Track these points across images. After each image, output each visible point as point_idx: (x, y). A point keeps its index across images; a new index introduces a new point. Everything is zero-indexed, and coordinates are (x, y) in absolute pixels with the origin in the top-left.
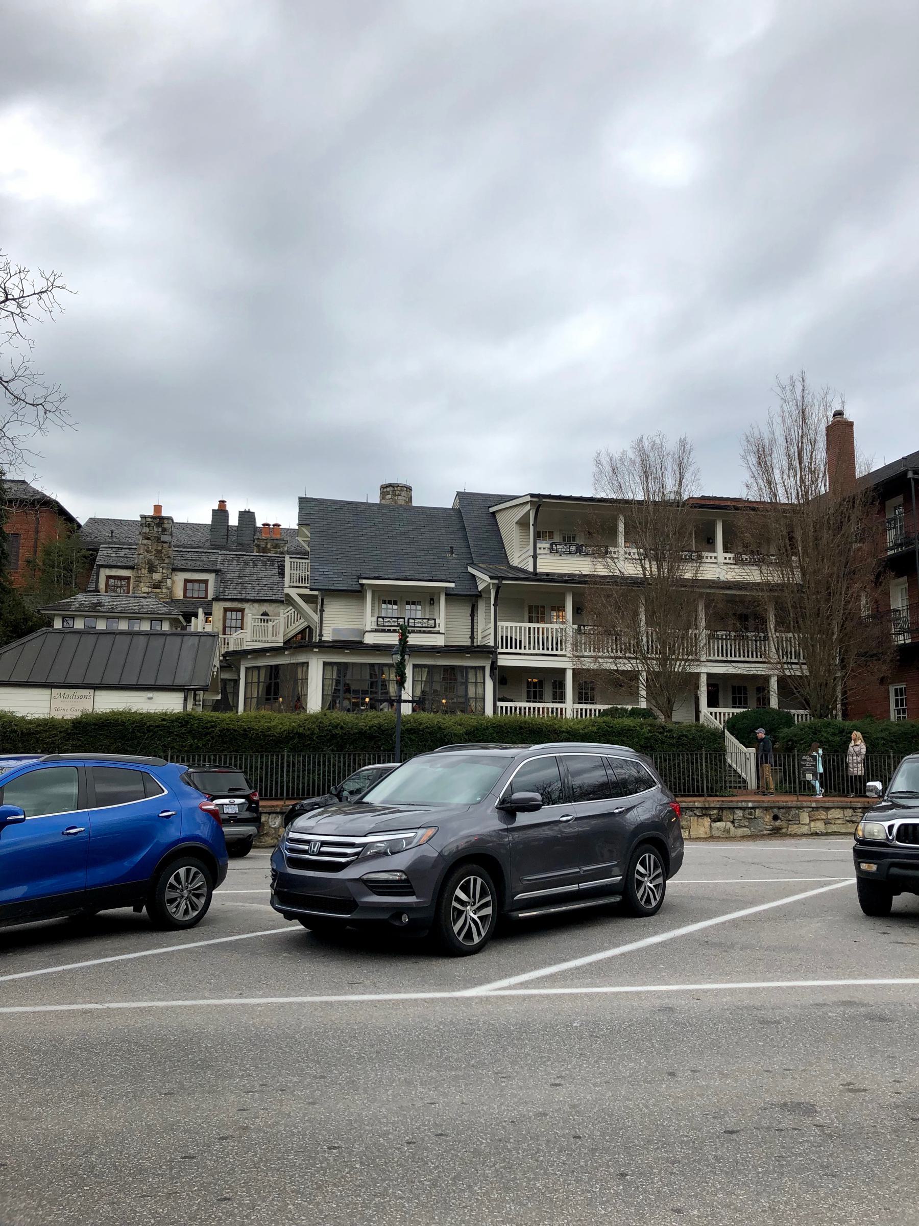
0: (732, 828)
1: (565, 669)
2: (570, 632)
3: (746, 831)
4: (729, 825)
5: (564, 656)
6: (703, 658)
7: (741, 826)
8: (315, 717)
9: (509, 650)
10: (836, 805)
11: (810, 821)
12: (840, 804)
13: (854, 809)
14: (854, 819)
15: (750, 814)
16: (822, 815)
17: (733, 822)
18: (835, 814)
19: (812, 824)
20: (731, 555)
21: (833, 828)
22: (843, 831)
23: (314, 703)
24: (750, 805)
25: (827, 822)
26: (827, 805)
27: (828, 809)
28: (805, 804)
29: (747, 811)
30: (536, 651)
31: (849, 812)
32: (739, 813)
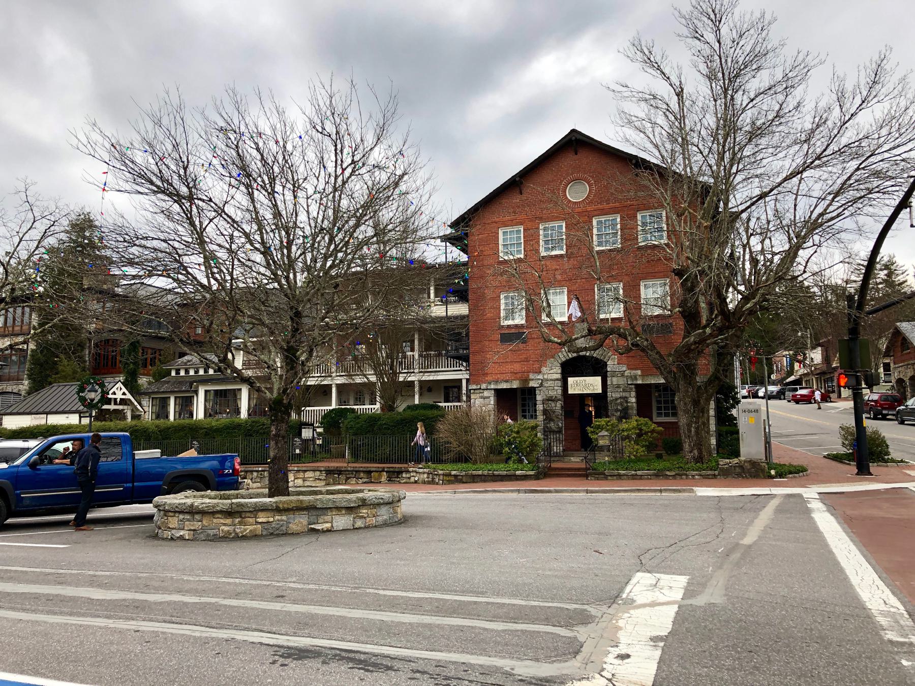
0: (251, 483)
2: (417, 357)
3: (259, 485)
5: (461, 370)
6: (334, 375)
8: (172, 424)
9: (443, 369)
10: (309, 469)
11: (295, 479)
12: (311, 468)
15: (261, 474)
16: (301, 475)
17: (252, 479)
18: (309, 474)
19: (296, 481)
23: (244, 414)
24: (260, 469)
25: (304, 480)
26: (304, 469)
27: (306, 471)
28: (255, 469)
30: (455, 369)
31: (318, 473)
32: (255, 474)
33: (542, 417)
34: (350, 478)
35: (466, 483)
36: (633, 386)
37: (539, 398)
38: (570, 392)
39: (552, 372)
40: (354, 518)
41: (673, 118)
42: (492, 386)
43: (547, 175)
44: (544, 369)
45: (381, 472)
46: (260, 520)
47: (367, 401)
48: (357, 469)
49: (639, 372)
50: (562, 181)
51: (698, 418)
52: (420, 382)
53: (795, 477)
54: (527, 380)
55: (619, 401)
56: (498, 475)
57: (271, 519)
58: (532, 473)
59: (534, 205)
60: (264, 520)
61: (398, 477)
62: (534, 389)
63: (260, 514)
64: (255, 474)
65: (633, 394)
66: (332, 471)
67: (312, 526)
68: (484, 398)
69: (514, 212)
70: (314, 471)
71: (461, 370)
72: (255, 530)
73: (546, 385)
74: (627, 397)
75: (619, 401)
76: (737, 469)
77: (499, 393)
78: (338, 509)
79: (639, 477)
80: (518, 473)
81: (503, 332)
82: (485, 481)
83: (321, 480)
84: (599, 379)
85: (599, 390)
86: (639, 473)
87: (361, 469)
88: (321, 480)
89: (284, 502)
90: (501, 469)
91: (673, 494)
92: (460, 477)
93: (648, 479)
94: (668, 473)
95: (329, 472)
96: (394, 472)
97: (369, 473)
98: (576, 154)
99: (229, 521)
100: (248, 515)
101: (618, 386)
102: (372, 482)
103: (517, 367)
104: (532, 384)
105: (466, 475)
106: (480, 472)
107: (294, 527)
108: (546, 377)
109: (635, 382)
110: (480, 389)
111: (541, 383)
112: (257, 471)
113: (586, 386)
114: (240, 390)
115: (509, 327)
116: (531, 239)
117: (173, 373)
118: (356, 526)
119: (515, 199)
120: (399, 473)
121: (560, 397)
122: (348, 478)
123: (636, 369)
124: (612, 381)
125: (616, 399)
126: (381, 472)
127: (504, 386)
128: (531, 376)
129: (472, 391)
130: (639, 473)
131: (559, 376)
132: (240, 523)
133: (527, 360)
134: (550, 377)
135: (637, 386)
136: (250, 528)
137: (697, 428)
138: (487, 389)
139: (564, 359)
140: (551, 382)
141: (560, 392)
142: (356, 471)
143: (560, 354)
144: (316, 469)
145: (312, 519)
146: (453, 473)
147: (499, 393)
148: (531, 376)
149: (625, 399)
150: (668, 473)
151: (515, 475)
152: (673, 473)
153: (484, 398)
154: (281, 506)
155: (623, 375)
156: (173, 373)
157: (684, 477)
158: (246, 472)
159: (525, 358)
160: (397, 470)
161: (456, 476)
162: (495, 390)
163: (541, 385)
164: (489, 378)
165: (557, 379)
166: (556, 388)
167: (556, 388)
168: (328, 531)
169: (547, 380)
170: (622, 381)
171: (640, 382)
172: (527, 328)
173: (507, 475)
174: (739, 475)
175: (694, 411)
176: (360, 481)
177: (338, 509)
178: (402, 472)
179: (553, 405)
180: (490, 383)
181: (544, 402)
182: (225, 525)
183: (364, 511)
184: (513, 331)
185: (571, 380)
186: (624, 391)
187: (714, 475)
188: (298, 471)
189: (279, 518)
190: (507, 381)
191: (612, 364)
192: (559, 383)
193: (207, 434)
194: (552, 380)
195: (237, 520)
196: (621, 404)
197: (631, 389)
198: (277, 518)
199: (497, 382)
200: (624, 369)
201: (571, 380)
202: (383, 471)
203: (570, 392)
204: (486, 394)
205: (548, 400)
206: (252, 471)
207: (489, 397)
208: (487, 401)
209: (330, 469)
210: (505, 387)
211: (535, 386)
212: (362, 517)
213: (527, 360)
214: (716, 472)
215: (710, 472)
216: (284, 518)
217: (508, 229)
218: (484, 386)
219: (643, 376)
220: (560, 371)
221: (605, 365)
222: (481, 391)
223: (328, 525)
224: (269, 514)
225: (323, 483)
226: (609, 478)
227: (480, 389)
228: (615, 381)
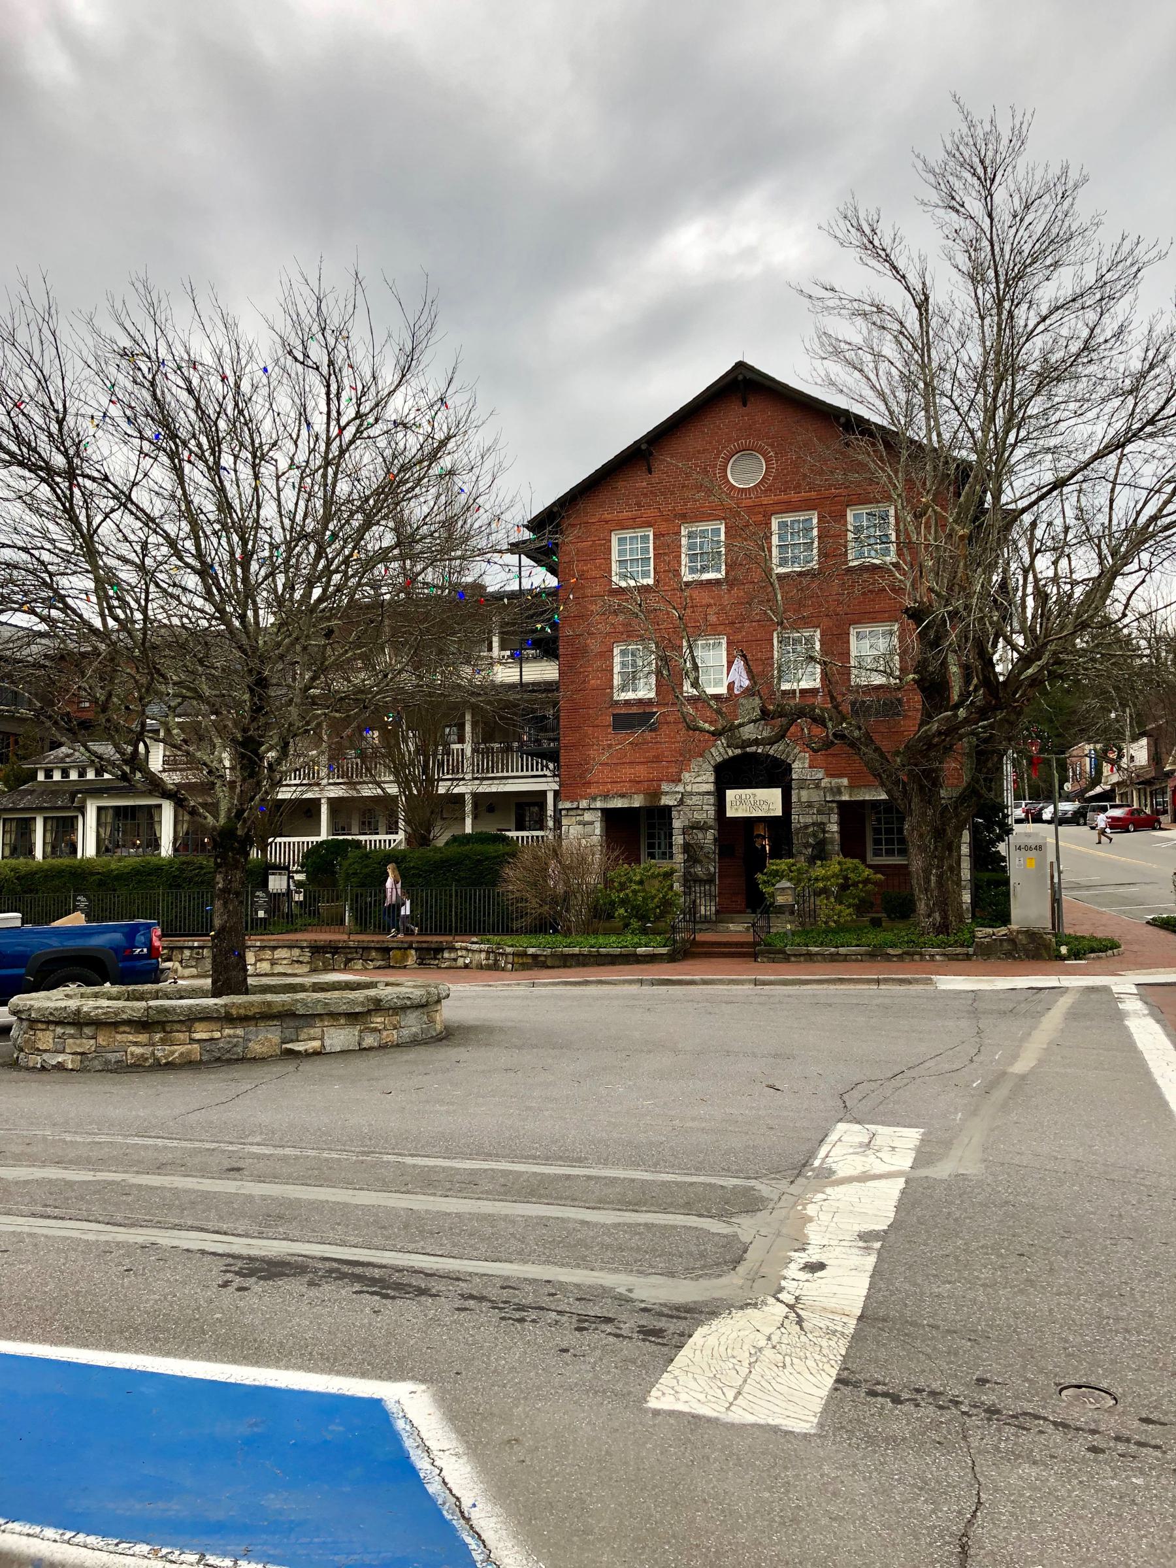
0: (180, 968)
1: (545, 792)
2: (468, 752)
3: (194, 971)
4: (177, 964)
5: (545, 776)
7: (187, 967)
9: (515, 774)
10: (281, 944)
11: (257, 961)
12: (287, 943)
13: (302, 948)
14: (301, 959)
15: (198, 954)
16: (268, 954)
17: (181, 962)
18: (281, 953)
19: (258, 964)
20: (508, 653)
21: (279, 969)
22: (290, 971)
23: (166, 849)
24: (196, 944)
25: (273, 963)
26: (272, 944)
27: (274, 948)
28: (186, 944)
29: (195, 951)
30: (535, 773)
31: (296, 952)
32: (187, 953)
33: (681, 856)
34: (353, 959)
35: (552, 967)
36: (834, 805)
37: (677, 824)
38: (730, 813)
39: (699, 779)
40: (361, 1031)
41: (910, 346)
42: (599, 804)
43: (693, 440)
44: (686, 776)
45: (406, 949)
46: (197, 1036)
47: (382, 828)
48: (365, 945)
49: (845, 781)
50: (719, 452)
51: (941, 859)
52: (475, 795)
53: (1099, 958)
54: (657, 794)
55: (811, 829)
56: (607, 955)
57: (217, 1035)
58: (664, 950)
59: (673, 493)
60: (205, 1036)
61: (436, 959)
62: (668, 809)
63: (198, 1026)
64: (187, 953)
65: (835, 818)
66: (323, 947)
67: (289, 1046)
68: (585, 824)
69: (638, 504)
70: (290, 947)
71: (545, 776)
72: (189, 1052)
73: (689, 802)
74: (824, 824)
75: (811, 829)
76: (1005, 944)
77: (608, 814)
78: (334, 1016)
79: (842, 958)
80: (640, 950)
81: (617, 711)
82: (584, 965)
83: (301, 963)
84: (777, 792)
85: (778, 812)
86: (842, 950)
87: (372, 945)
88: (301, 963)
89: (239, 1006)
90: (611, 945)
91: (898, 987)
92: (543, 959)
93: (856, 961)
94: (890, 951)
95: (317, 950)
96: (428, 949)
97: (384, 951)
98: (745, 405)
99: (143, 1038)
100: (177, 1027)
101: (810, 805)
102: (390, 967)
103: (641, 771)
104: (666, 801)
105: (553, 955)
106: (576, 950)
107: (256, 1048)
108: (689, 788)
109: (837, 798)
110: (578, 808)
111: (681, 799)
112: (191, 948)
113: (755, 805)
114: (160, 806)
115: (627, 703)
116: (667, 553)
117: (41, 777)
118: (365, 1045)
119: (640, 482)
120: (439, 950)
121: (711, 822)
122: (349, 961)
123: (840, 776)
124: (801, 796)
125: (806, 827)
126: (406, 949)
127: (618, 803)
128: (665, 787)
129: (563, 812)
130: (842, 950)
131: (710, 787)
132: (163, 1041)
133: (657, 759)
134: (696, 789)
135: (842, 805)
136: (180, 1049)
137: (940, 877)
138: (589, 809)
139: (719, 759)
140: (698, 797)
141: (712, 814)
142: (364, 949)
143: (713, 750)
144: (294, 944)
145: (289, 1033)
146: (531, 951)
147: (608, 814)
148: (665, 787)
149: (822, 826)
150: (890, 951)
151: (635, 955)
152: (899, 951)
153: (585, 824)
154: (234, 1012)
155: (817, 786)
156: (41, 777)
157: (917, 957)
158: (172, 949)
159: (657, 757)
160: (433, 946)
161: (535, 956)
162: (603, 810)
163: (681, 802)
164: (593, 790)
165: (708, 793)
166: (705, 807)
167: (705, 807)
168: (317, 1053)
169: (691, 794)
170: (815, 796)
171: (845, 798)
172: (659, 704)
173: (621, 955)
174: (1009, 955)
175: (936, 848)
176: (371, 965)
177: (334, 1016)
178: (442, 950)
179: (700, 836)
180: (594, 799)
181: (684, 831)
182: (136, 1044)
183: (378, 1020)
184: (634, 710)
185: (730, 794)
186: (820, 812)
187: (967, 954)
188: (262, 948)
189: (231, 1032)
190: (623, 796)
191: (800, 768)
192: (712, 799)
193: (101, 884)
194: (699, 794)
195: (158, 1037)
196: (814, 835)
197: (831, 809)
198: (227, 1032)
199: (606, 797)
200: (820, 776)
201: (730, 794)
202: (410, 947)
203: (730, 813)
204: (588, 817)
205: (693, 828)
206: (182, 948)
207: (592, 823)
208: (589, 828)
209: (318, 944)
210: (620, 806)
211: (671, 803)
212: (375, 1030)
213: (657, 759)
214: (971, 950)
215: (959, 950)
216: (240, 1032)
217: (627, 534)
218: (584, 804)
219: (851, 787)
220: (712, 779)
221: (789, 769)
222: (580, 812)
223: (316, 1044)
224: (213, 1026)
225: (306, 968)
226: (793, 959)
227: (578, 808)
228: (804, 794)
